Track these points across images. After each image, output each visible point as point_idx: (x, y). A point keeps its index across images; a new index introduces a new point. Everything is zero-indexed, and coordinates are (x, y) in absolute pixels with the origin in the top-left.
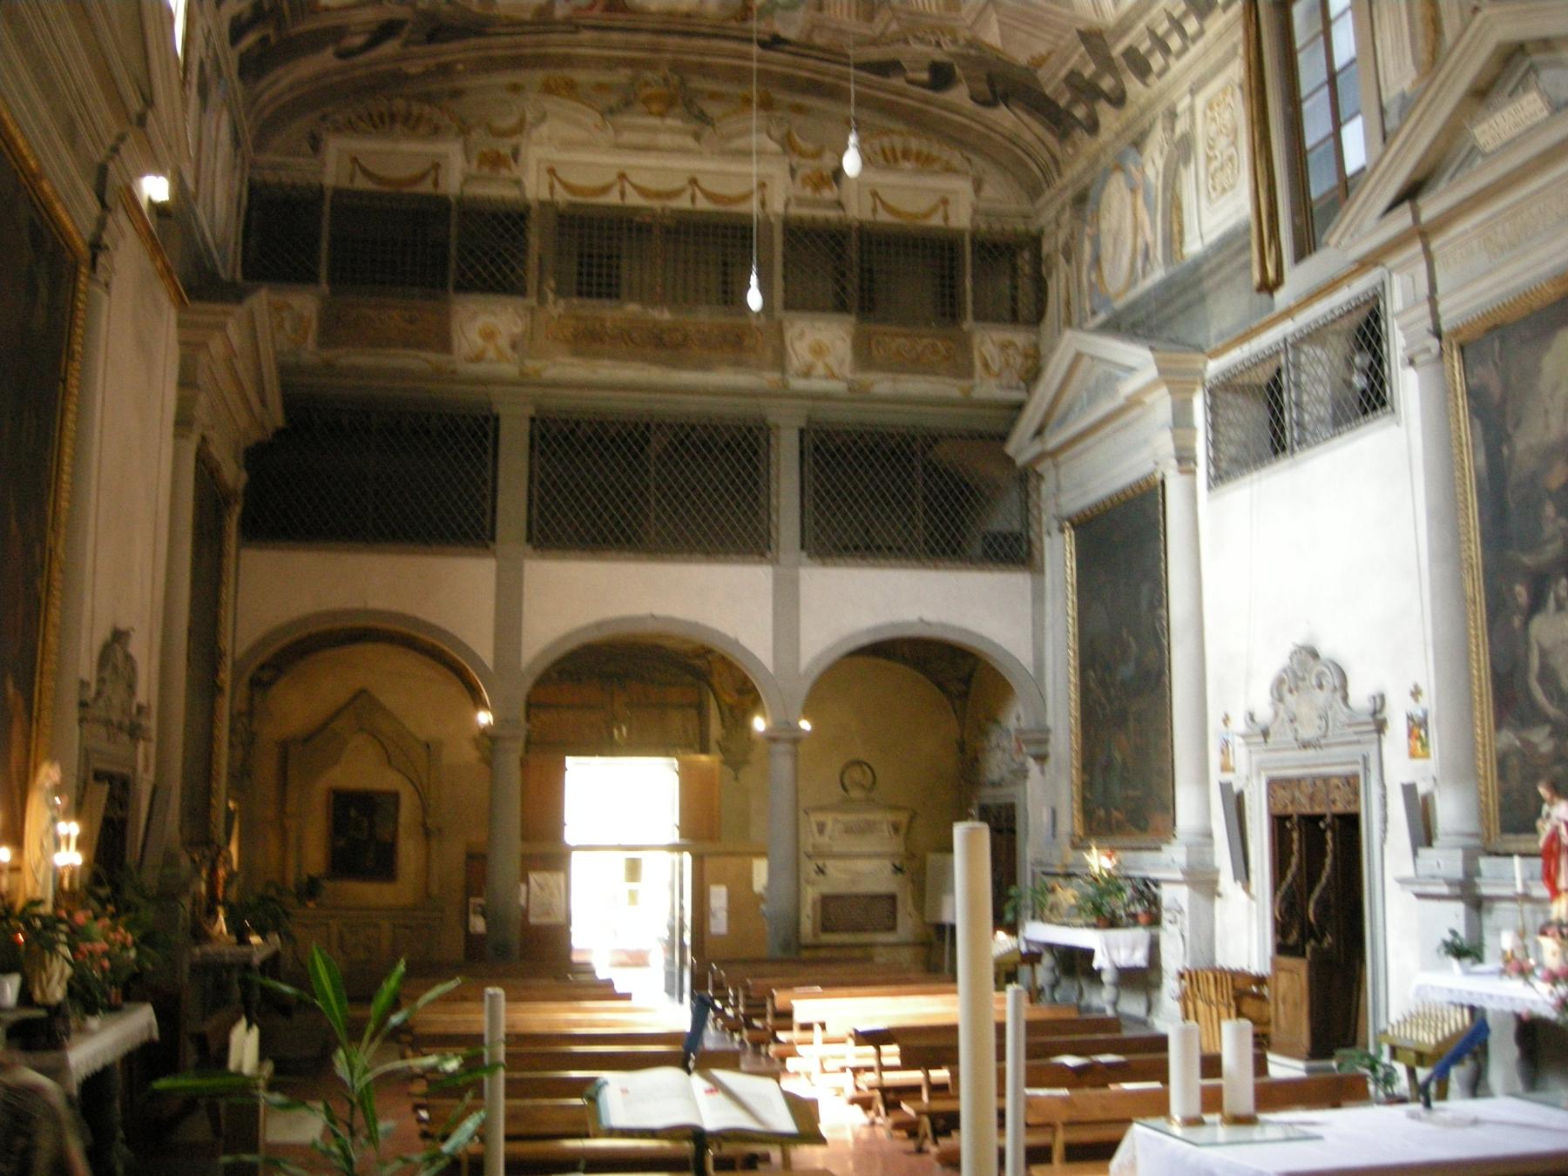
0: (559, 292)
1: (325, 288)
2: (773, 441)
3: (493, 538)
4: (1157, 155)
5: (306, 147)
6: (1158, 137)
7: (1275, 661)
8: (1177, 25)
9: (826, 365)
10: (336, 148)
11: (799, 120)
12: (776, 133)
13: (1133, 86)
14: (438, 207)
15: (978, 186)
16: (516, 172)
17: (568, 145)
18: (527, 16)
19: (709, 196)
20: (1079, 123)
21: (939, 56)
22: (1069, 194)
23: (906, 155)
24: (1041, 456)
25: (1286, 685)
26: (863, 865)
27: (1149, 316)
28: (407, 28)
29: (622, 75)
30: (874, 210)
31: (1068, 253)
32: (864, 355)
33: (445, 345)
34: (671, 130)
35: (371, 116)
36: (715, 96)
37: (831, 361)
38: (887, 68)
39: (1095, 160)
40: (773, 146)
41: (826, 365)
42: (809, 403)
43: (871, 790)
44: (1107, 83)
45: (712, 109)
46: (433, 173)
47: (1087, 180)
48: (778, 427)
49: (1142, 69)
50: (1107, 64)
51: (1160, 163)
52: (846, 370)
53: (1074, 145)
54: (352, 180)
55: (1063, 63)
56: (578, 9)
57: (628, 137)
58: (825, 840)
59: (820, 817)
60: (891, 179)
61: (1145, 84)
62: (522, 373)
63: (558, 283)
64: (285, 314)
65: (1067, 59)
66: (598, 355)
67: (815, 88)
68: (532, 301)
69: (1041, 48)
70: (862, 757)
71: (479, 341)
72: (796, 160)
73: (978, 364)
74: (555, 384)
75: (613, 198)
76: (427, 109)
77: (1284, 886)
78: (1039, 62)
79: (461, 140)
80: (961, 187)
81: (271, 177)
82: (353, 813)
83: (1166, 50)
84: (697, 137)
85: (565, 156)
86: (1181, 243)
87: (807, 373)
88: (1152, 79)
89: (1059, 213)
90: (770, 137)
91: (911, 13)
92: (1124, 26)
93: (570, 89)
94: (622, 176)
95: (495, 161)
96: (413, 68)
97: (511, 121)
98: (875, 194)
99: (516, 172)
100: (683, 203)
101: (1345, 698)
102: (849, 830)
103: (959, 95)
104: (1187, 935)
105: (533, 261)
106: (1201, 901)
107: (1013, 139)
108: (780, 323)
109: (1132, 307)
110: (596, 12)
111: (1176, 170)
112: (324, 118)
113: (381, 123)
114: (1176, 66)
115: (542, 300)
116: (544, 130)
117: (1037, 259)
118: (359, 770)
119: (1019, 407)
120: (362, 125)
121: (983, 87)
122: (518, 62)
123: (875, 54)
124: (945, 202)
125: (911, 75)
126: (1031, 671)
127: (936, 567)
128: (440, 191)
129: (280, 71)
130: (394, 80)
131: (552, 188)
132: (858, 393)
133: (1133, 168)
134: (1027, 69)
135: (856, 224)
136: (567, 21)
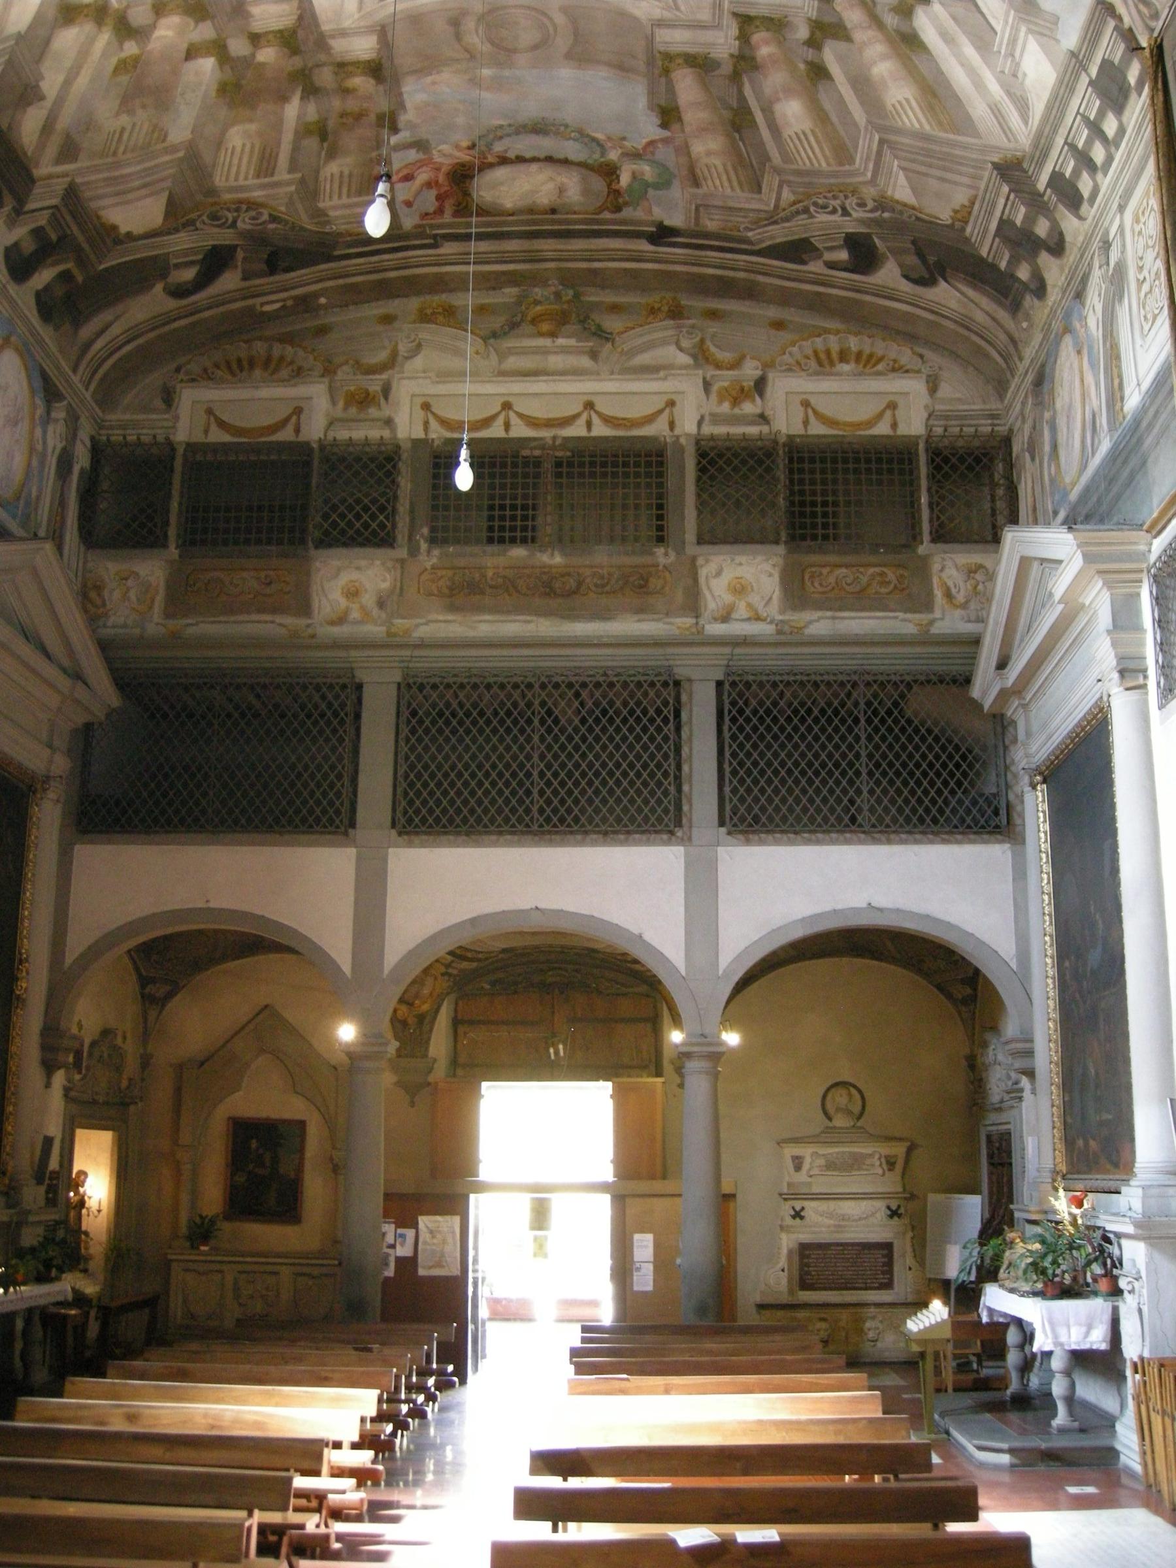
0: (433, 541)
1: (173, 551)
3: (353, 824)
4: (1096, 298)
5: (158, 403)
8: (1096, 129)
10: (190, 398)
11: (713, 328)
13: (1070, 224)
15: (933, 389)
16: (386, 412)
17: (445, 376)
19: (607, 420)
22: (1030, 378)
23: (843, 357)
24: (1004, 695)
26: (850, 1208)
27: (1099, 501)
28: (240, 255)
29: (510, 293)
30: (806, 423)
31: (1033, 448)
32: (796, 592)
33: (305, 609)
34: (565, 350)
35: (228, 363)
36: (615, 308)
37: (755, 599)
38: (798, 250)
42: (727, 650)
43: (859, 1118)
44: (1042, 228)
45: (612, 323)
46: (294, 418)
48: (690, 680)
49: (1074, 201)
51: (1099, 308)
52: (774, 610)
53: (1028, 317)
54: (206, 432)
55: (991, 213)
57: (512, 362)
58: (802, 1177)
59: (797, 1150)
60: (828, 385)
61: (1080, 218)
62: (389, 634)
63: (433, 530)
64: (130, 583)
65: (994, 205)
66: (479, 609)
67: (725, 288)
68: (402, 553)
69: (960, 197)
71: (343, 602)
72: (711, 372)
73: (938, 593)
74: (421, 645)
76: (289, 350)
78: (963, 215)
79: (326, 380)
80: (913, 388)
81: (116, 438)
82: (254, 1144)
84: (594, 355)
85: (442, 389)
86: (1122, 399)
87: (725, 618)
88: (1085, 207)
89: (1023, 404)
90: (681, 350)
91: (799, 173)
93: (450, 315)
94: (507, 406)
95: (363, 400)
97: (383, 356)
98: (806, 404)
99: (386, 412)
100: (577, 430)
103: (889, 274)
105: (403, 507)
107: (966, 324)
108: (694, 559)
110: (447, 218)
112: (178, 370)
113: (239, 369)
114: (1105, 182)
115: (414, 551)
116: (418, 362)
117: (1010, 465)
118: (263, 1097)
120: (220, 373)
121: (912, 260)
122: (384, 290)
123: (779, 234)
124: (892, 406)
125: (829, 256)
126: (1014, 966)
127: (889, 842)
128: (302, 438)
130: (250, 322)
131: (426, 424)
132: (787, 637)
135: (782, 440)
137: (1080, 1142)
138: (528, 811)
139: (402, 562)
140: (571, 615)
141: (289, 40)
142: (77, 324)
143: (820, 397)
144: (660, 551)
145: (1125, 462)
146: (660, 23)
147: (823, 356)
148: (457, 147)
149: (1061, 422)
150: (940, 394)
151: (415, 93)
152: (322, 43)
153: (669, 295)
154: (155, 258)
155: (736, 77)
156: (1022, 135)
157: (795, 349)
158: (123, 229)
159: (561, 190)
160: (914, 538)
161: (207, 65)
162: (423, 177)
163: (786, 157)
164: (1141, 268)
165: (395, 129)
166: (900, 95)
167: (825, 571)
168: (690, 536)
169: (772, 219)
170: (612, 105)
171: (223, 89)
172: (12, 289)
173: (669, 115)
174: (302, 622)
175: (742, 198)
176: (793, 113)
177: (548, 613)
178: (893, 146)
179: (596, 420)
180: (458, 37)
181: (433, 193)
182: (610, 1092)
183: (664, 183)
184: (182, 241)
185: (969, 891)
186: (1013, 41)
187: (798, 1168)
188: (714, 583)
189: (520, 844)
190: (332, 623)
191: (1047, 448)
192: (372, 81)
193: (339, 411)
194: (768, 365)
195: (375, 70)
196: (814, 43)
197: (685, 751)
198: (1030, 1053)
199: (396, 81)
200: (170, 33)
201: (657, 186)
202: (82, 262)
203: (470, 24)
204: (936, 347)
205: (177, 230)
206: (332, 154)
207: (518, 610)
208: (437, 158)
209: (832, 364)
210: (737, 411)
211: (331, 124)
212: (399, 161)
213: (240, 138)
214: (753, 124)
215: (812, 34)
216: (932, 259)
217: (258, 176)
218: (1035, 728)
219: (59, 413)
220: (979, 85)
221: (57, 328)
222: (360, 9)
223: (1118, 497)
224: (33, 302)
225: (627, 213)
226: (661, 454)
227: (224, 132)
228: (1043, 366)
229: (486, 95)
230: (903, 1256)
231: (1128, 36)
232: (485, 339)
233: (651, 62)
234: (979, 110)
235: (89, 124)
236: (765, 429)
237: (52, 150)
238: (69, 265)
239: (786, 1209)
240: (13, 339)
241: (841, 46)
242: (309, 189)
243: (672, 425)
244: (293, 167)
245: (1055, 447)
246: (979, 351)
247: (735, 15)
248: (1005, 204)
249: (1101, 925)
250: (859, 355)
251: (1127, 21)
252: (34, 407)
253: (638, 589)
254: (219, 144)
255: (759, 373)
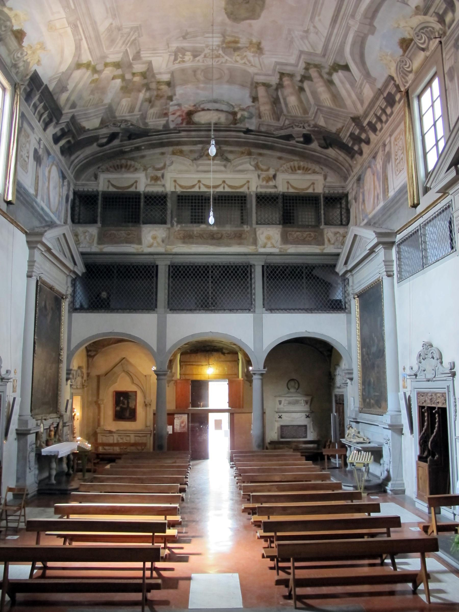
0: (179, 222)
1: (99, 225)
2: (253, 270)
3: (156, 307)
4: (380, 161)
5: (93, 178)
6: (380, 154)
7: (418, 348)
8: (384, 111)
9: (272, 243)
11: (260, 159)
12: (253, 163)
13: (372, 136)
14: (136, 196)
15: (325, 179)
17: (181, 172)
18: (161, 128)
19: (230, 186)
20: (356, 152)
21: (305, 132)
22: (356, 178)
23: (299, 168)
24: (346, 272)
25: (421, 357)
26: (294, 415)
27: (379, 220)
28: (120, 135)
30: (288, 188)
31: (356, 199)
32: (285, 239)
33: (140, 243)
34: (216, 165)
36: (231, 152)
37: (273, 241)
38: (289, 137)
39: (362, 165)
40: (252, 168)
41: (272, 243)
42: (265, 256)
44: (363, 136)
45: (230, 156)
46: (135, 184)
47: (360, 173)
48: (254, 265)
49: (374, 130)
50: (363, 129)
51: (381, 163)
52: (279, 244)
53: (356, 160)
54: (108, 187)
55: (348, 130)
56: (177, 124)
57: (201, 168)
58: (281, 406)
61: (376, 135)
62: (166, 251)
63: (178, 219)
64: (87, 234)
65: (349, 128)
66: (192, 243)
68: (169, 226)
69: (339, 126)
70: (294, 378)
71: (152, 241)
72: (260, 172)
73: (326, 240)
75: (196, 189)
76: (133, 163)
77: (422, 433)
78: (339, 131)
81: (81, 189)
82: (122, 398)
83: (381, 121)
84: (225, 166)
85: (180, 176)
86: (388, 192)
87: (264, 247)
88: (378, 133)
89: (353, 185)
91: (292, 116)
92: (366, 114)
94: (199, 181)
95: (156, 179)
96: (127, 149)
97: (162, 165)
98: (288, 183)
99: (163, 182)
100: (220, 189)
101: (441, 363)
102: (289, 403)
103: (315, 145)
104: (391, 449)
105: (169, 212)
106: (396, 436)
107: (336, 160)
108: (255, 229)
109: (374, 217)
110: (184, 125)
111: (386, 166)
112: (99, 168)
113: (118, 168)
114: (385, 126)
115: (172, 225)
116: (172, 167)
117: (347, 202)
118: (124, 385)
119: (338, 255)
120: (111, 169)
121: (322, 142)
122: (162, 145)
123: (283, 133)
124: (313, 184)
125: (297, 139)
126: (347, 348)
128: (138, 190)
129: (79, 153)
131: (175, 186)
133: (373, 166)
134: (335, 133)
135: (281, 193)
136: (175, 129)
137: (368, 400)
138: (208, 303)
139: (169, 229)
140: (219, 245)
141: (143, 75)
142: (71, 155)
143: (291, 180)
144: (245, 226)
145: (388, 210)
146: (257, 74)
147: (293, 168)
148: (190, 106)
149: (366, 193)
150: (327, 180)
151: (179, 91)
152: (154, 76)
153: (247, 148)
154: (96, 136)
155: (277, 89)
156: (360, 110)
157: (285, 166)
158: (87, 128)
159: (219, 119)
160: (319, 223)
161: (118, 82)
162: (178, 113)
163: (288, 112)
164: (396, 155)
165: (172, 100)
166: (325, 97)
167: (293, 233)
168: (254, 222)
169: (281, 128)
170: (238, 96)
171: (122, 88)
172: (54, 146)
173: (255, 99)
174: (139, 246)
175: (274, 123)
176: (292, 100)
177: (212, 245)
178: (321, 111)
179: (226, 186)
180: (195, 75)
181: (180, 118)
182: (227, 382)
183: (250, 117)
184: (105, 131)
185: (337, 329)
186: (361, 84)
187: (280, 403)
188: (261, 236)
189: (205, 313)
190: (149, 247)
191: (361, 200)
192: (167, 87)
193: (149, 182)
194: (277, 170)
195: (169, 84)
196: (302, 81)
197: (253, 286)
198: (352, 373)
199: (174, 87)
200: (108, 72)
201: (248, 118)
202: (74, 137)
203: (199, 72)
204: (327, 166)
205: (102, 128)
206: (152, 107)
207: (204, 244)
208: (183, 109)
209: (296, 170)
210: (267, 184)
211: (153, 99)
212: (172, 109)
213: (125, 102)
214: (280, 103)
215: (301, 79)
216: (328, 142)
217: (129, 112)
218: (356, 282)
219: (66, 183)
220: (349, 95)
221: (65, 157)
222: (167, 65)
223: (385, 220)
224: (59, 150)
225: (238, 125)
226: (245, 197)
227: (121, 100)
228: (360, 176)
229: (200, 92)
230: (310, 429)
231: (397, 87)
232: (192, 160)
233: (252, 84)
234: (348, 102)
235: (80, 98)
236: (276, 190)
237: (69, 105)
238: (70, 139)
239: (277, 415)
240: (55, 162)
241: (310, 82)
242: (144, 117)
243: (248, 188)
244: (140, 110)
245: (364, 201)
246: (339, 167)
247: (279, 72)
248: (353, 128)
249: (376, 341)
250: (304, 167)
251: (397, 82)
252: (60, 181)
253: (239, 237)
254: (118, 104)
255: (274, 173)
